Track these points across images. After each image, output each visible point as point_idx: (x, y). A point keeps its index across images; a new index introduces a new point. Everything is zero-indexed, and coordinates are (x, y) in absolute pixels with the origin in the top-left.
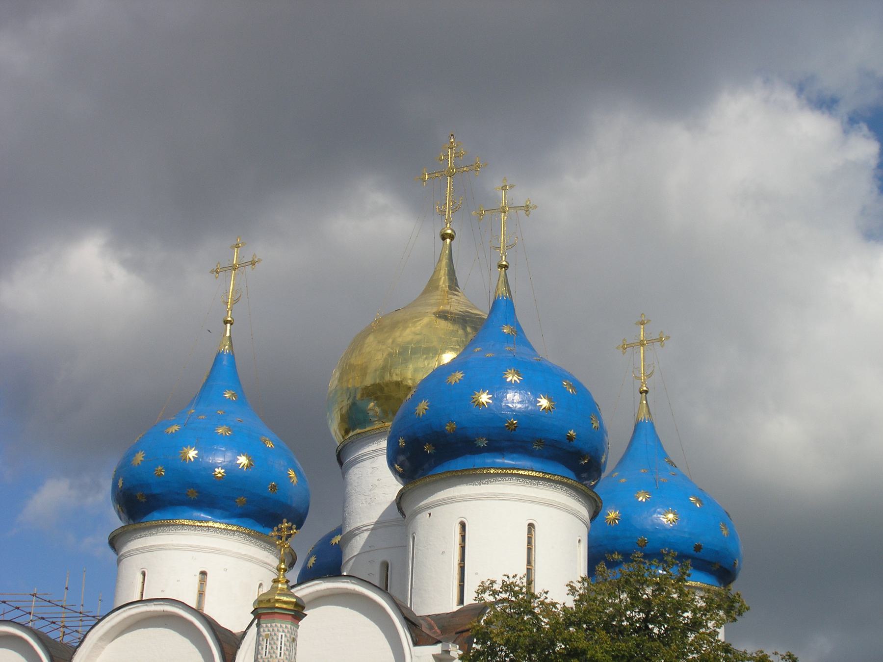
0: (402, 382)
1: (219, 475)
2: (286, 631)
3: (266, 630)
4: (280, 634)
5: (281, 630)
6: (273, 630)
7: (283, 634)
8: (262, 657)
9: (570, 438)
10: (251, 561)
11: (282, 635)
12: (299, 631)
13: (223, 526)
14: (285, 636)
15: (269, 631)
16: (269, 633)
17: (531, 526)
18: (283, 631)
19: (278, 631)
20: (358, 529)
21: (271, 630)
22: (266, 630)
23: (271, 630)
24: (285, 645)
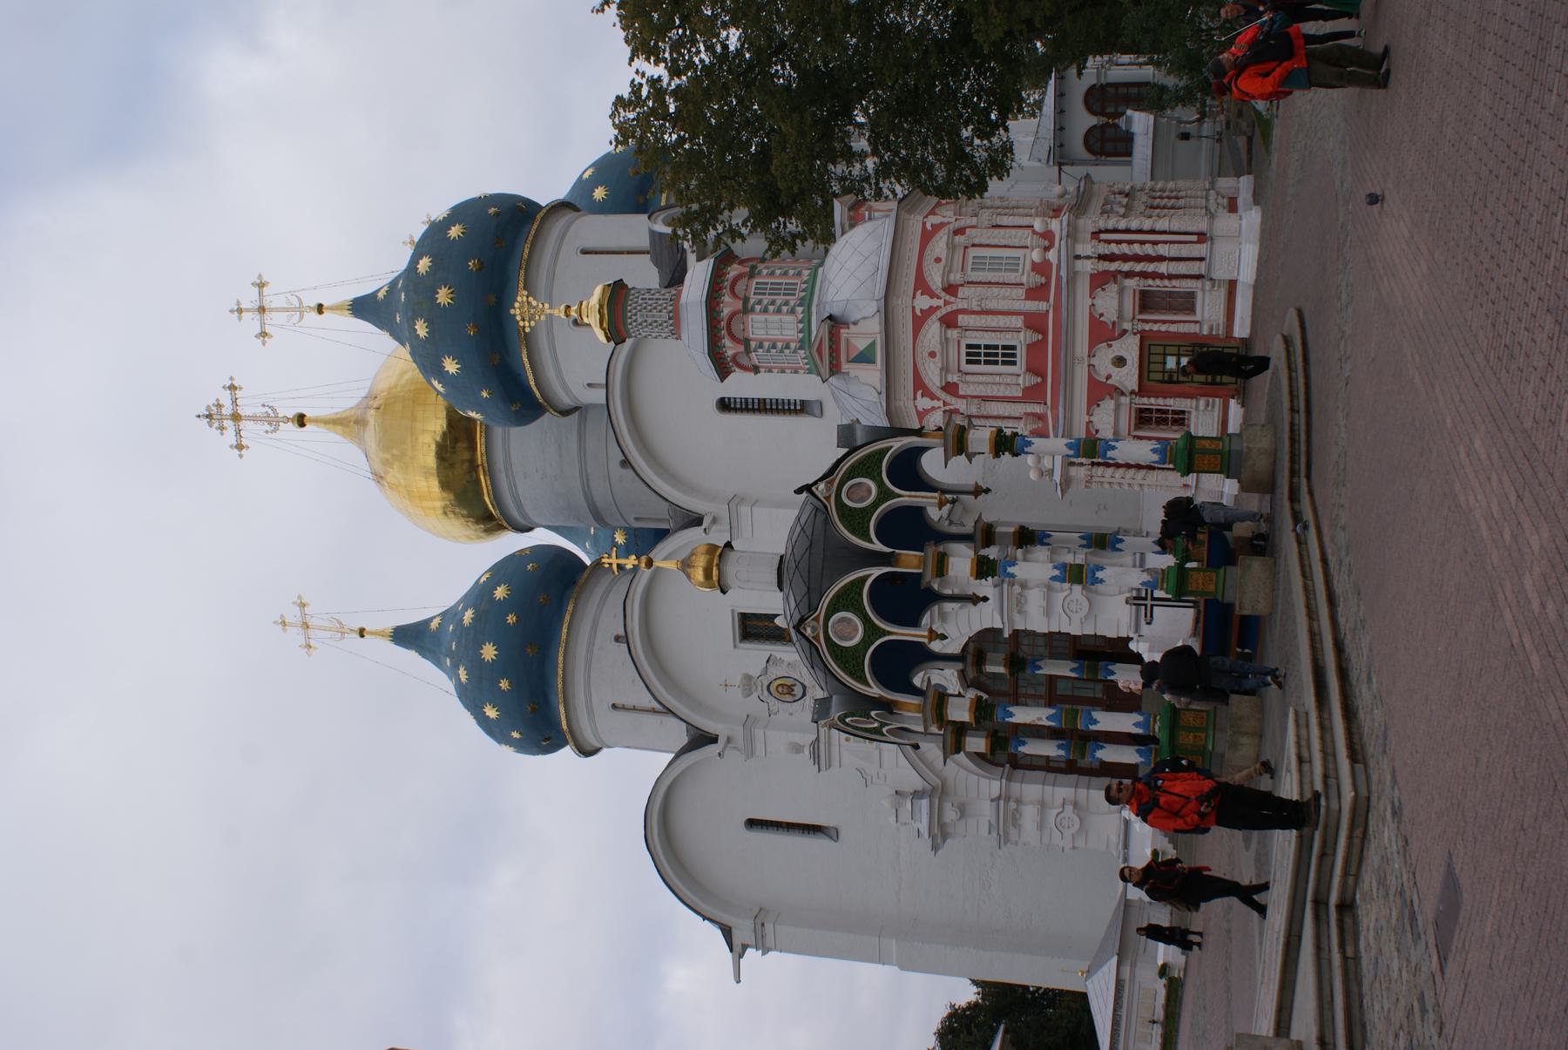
0: (436, 442)
1: (514, 618)
2: (637, 295)
3: (634, 318)
4: (640, 302)
5: (636, 300)
6: (635, 308)
8: (666, 322)
9: (497, 214)
10: (609, 593)
11: (642, 299)
12: (639, 286)
13: (568, 617)
14: (643, 295)
15: (635, 314)
16: (639, 313)
17: (585, 252)
18: (638, 297)
19: (636, 303)
20: (586, 496)
21: (634, 311)
22: (634, 318)
23: (634, 311)
24: (653, 295)
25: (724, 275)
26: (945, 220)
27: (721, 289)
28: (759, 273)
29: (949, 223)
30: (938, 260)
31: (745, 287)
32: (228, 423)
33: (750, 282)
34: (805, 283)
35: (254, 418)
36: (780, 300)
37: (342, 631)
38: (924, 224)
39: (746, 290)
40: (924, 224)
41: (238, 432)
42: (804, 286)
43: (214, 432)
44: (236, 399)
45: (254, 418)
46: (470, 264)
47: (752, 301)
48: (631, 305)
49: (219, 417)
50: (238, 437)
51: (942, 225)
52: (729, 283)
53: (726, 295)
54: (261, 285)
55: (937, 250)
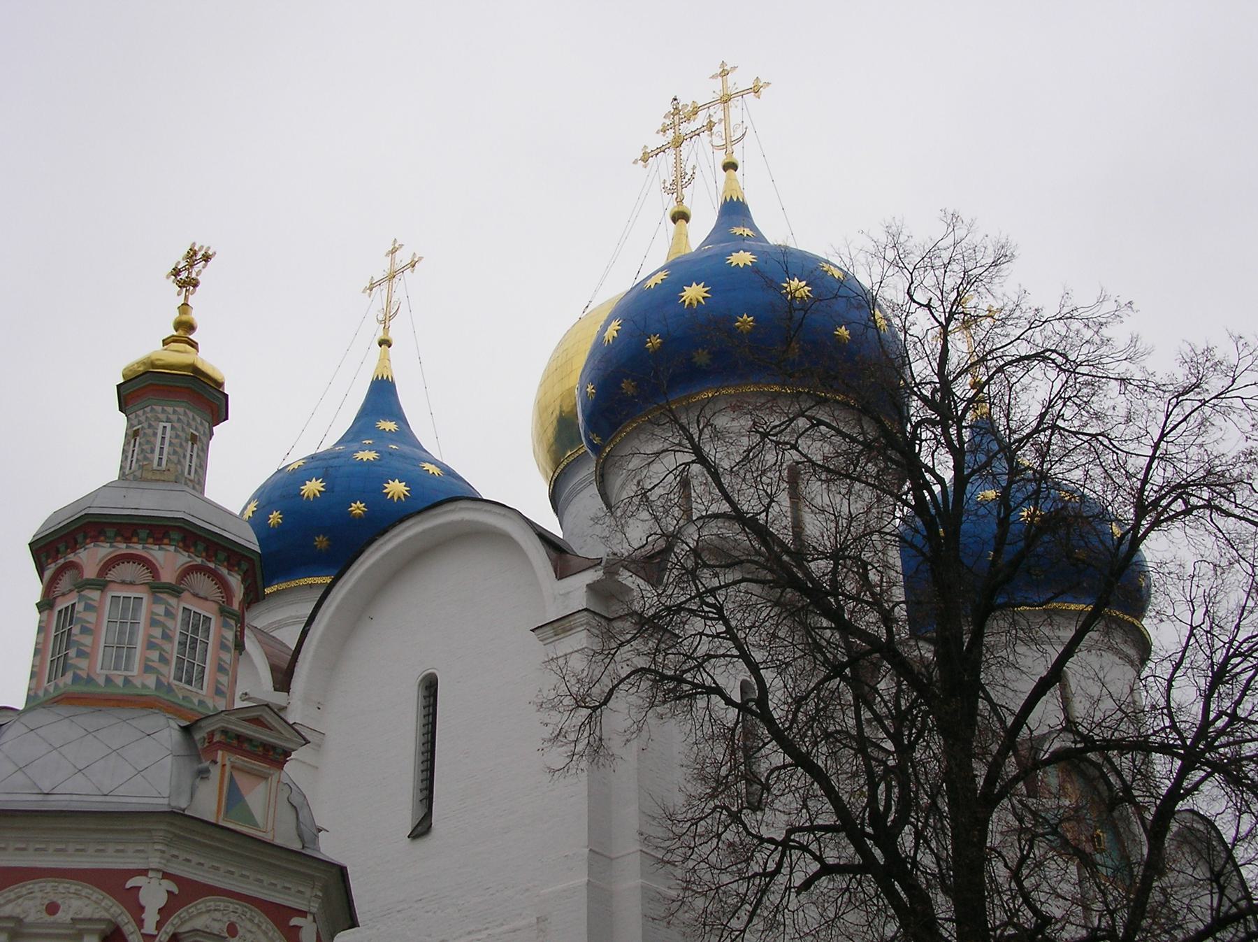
1: (358, 511)
7: (169, 425)
14: (173, 428)
24: (171, 444)
25: (158, 541)
26: (151, 918)
27: (127, 540)
28: (156, 601)
29: (140, 923)
30: (52, 908)
31: (128, 579)
32: (670, 134)
33: (146, 588)
34: (127, 681)
35: (678, 161)
36: (173, 650)
37: (385, 322)
38: (143, 872)
39: (123, 583)
40: (143, 872)
41: (662, 150)
42: (120, 682)
43: (659, 121)
44: (698, 135)
45: (678, 161)
46: (745, 316)
47: (95, 595)
48: (185, 414)
49: (677, 122)
50: (659, 150)
51: (137, 910)
52: (144, 554)
53: (111, 550)
54: (756, 91)
55: (76, 904)
